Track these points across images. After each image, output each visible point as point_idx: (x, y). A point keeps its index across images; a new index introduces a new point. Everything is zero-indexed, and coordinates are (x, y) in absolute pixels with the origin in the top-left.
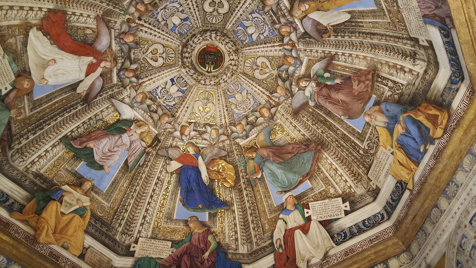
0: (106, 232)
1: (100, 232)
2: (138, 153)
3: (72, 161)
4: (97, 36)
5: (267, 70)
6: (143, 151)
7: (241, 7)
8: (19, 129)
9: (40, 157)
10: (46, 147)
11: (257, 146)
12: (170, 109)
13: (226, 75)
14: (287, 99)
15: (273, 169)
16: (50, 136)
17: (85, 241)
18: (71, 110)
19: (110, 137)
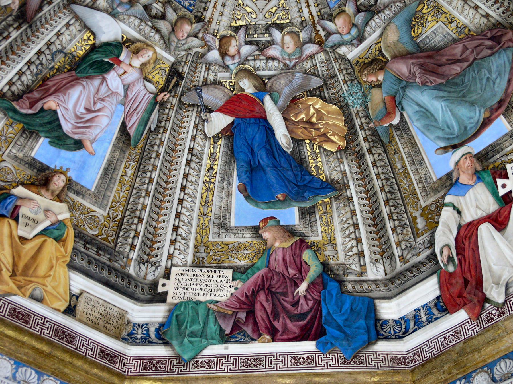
0: (108, 262)
1: (98, 263)
2: (143, 106)
3: (22, 140)
6: (154, 102)
11: (384, 56)
12: (190, 5)
15: (426, 102)
17: (72, 282)
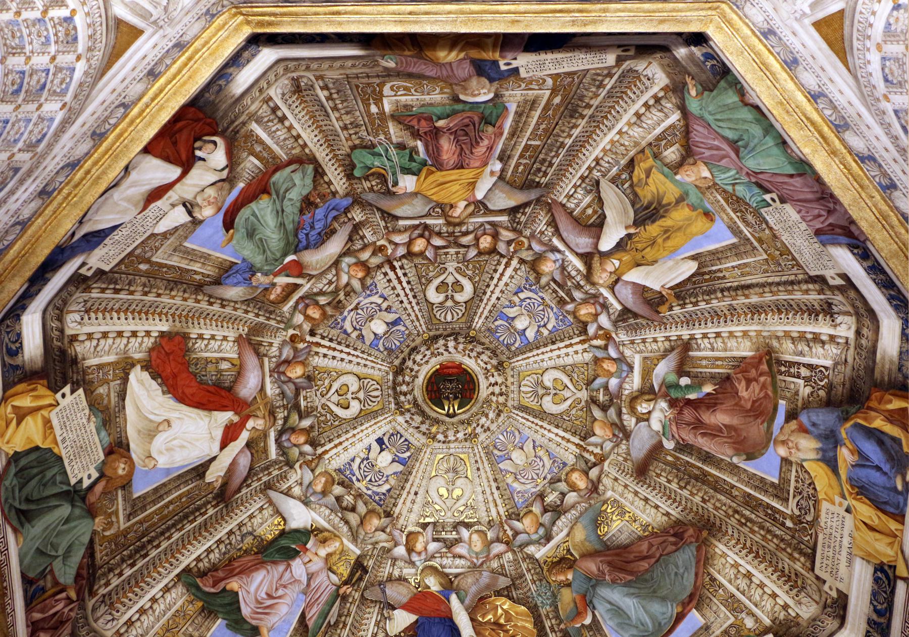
2: (324, 598)
3: (200, 618)
4: (239, 373)
5: (567, 394)
7: (496, 286)
8: (107, 555)
9: (142, 611)
10: (153, 592)
11: (572, 555)
12: (380, 500)
13: (487, 416)
14: (618, 445)
16: (160, 569)
18: (195, 518)
19: (269, 568)
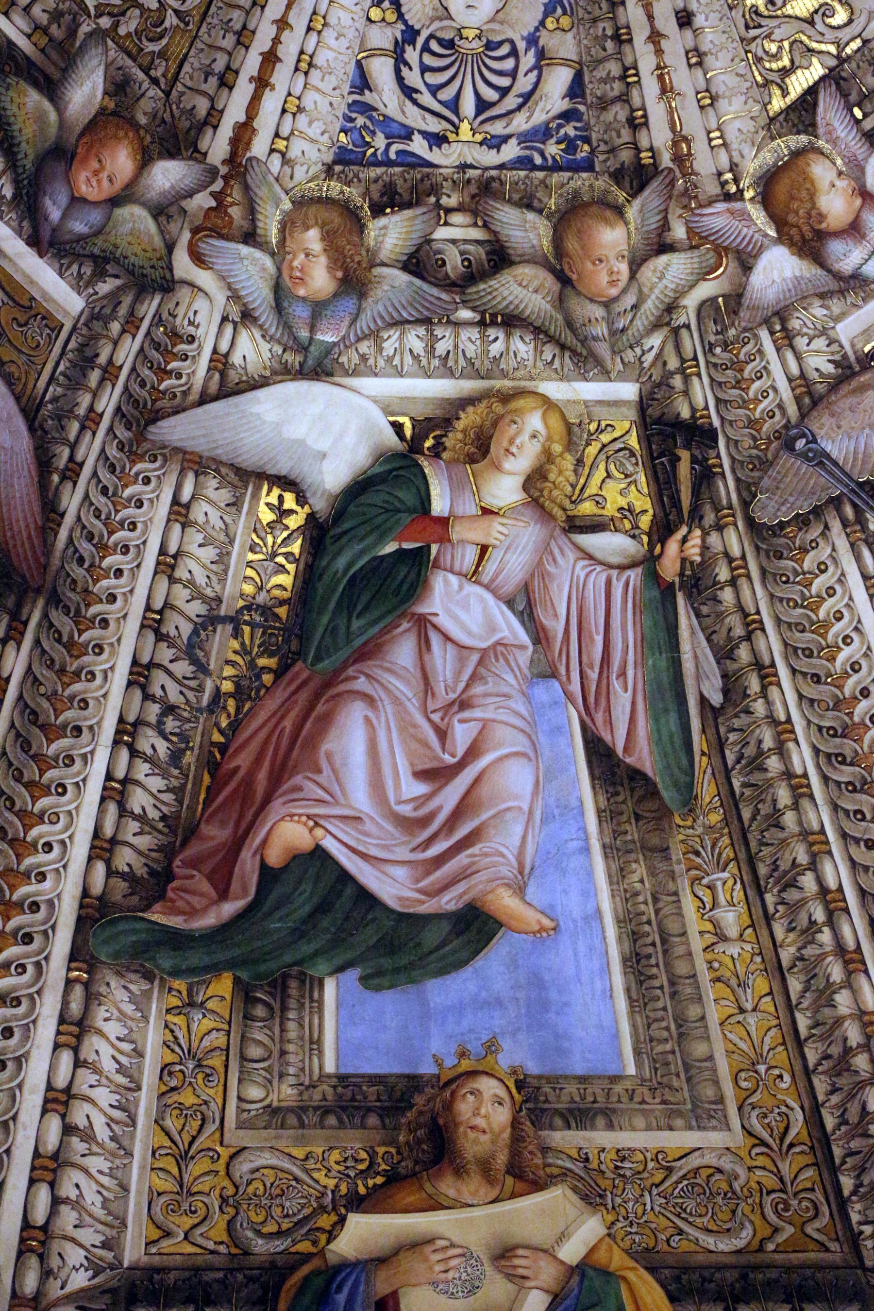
6: (656, 593)
12: (571, 146)
